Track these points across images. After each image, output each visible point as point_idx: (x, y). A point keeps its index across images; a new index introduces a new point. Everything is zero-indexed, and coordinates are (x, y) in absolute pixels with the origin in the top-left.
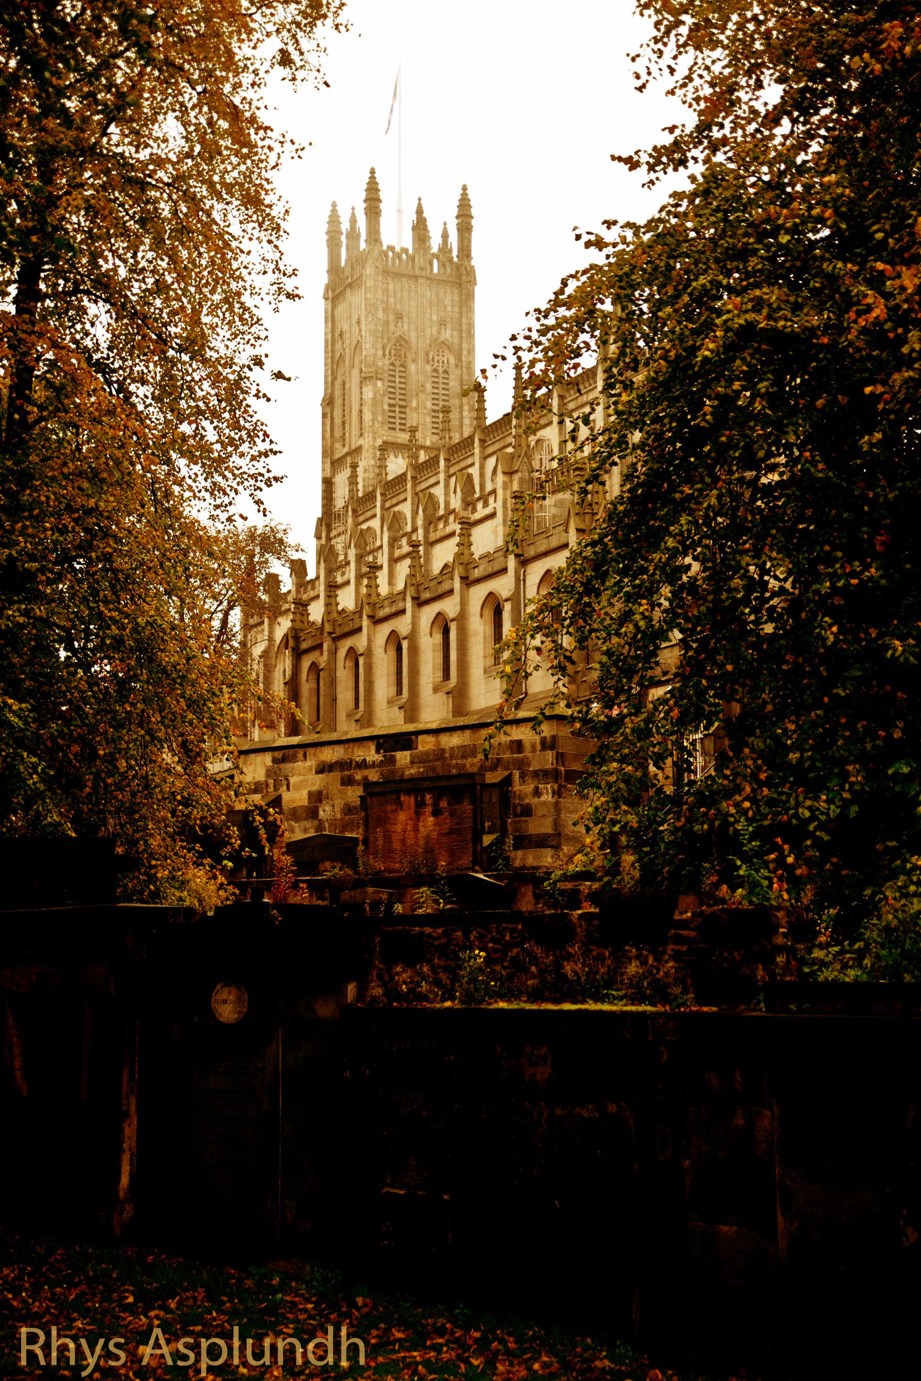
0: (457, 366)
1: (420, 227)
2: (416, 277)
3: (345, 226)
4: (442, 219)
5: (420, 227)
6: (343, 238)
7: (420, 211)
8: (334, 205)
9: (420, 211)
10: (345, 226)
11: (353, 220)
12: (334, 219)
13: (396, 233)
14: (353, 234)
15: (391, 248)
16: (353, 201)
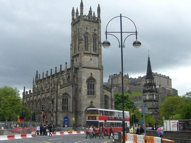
0: (98, 38)
1: (90, 12)
2: (90, 21)
3: (75, 11)
4: (95, 10)
6: (75, 14)
7: (91, 9)
8: (73, 8)
9: (91, 9)
10: (75, 11)
11: (77, 10)
12: (73, 10)
13: (86, 12)
14: (77, 13)
15: (85, 15)
16: (77, 6)
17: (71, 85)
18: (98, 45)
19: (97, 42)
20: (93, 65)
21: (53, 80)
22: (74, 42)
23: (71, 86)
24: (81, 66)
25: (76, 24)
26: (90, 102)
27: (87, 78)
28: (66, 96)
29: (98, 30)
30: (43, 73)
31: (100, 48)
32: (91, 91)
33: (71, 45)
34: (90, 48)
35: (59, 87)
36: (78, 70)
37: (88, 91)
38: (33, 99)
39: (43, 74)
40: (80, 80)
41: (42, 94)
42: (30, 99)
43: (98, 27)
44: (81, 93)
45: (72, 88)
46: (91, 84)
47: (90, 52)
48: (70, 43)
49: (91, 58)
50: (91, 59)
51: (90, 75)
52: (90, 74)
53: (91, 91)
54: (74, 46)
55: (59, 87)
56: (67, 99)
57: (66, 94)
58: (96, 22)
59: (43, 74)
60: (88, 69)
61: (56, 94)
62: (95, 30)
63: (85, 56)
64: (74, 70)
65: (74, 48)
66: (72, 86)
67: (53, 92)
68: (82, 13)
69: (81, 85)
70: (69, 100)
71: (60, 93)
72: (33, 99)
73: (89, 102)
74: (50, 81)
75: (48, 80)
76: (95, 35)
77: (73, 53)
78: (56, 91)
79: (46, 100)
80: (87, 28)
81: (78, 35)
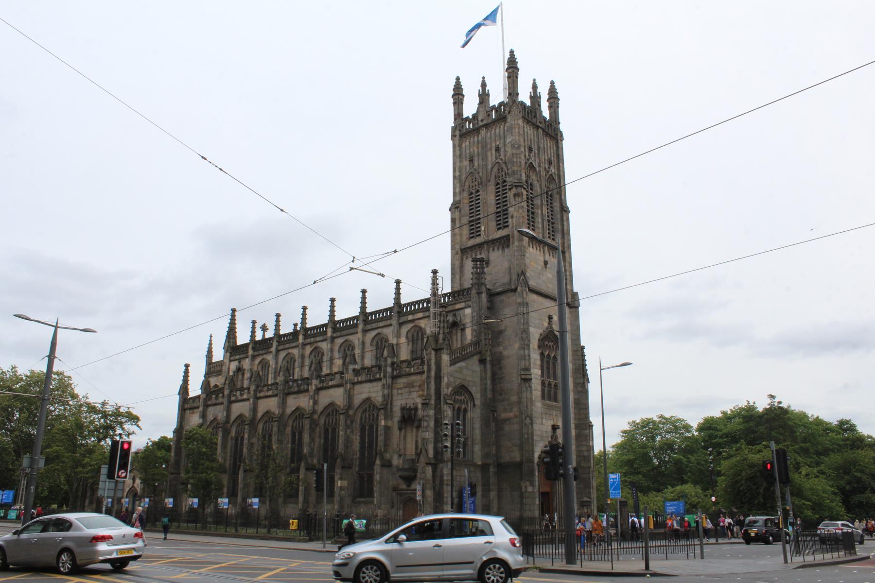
1: (535, 97)
2: (538, 127)
5: (535, 97)
13: (524, 96)
17: (476, 358)
18: (559, 216)
19: (556, 205)
20: (550, 286)
21: (339, 341)
22: (466, 194)
23: (477, 362)
24: (526, 283)
25: (483, 132)
26: (550, 428)
27: (540, 331)
28: (463, 398)
29: (559, 166)
30: (254, 322)
31: (565, 228)
32: (550, 384)
33: (455, 207)
34: (540, 220)
35: (445, 358)
36: (503, 297)
37: (543, 383)
38: (255, 409)
39: (254, 328)
40: (524, 335)
41: (318, 389)
42: (228, 411)
43: (558, 155)
44: (531, 387)
45: (477, 368)
46: (549, 355)
47: (541, 235)
48: (450, 201)
49: (547, 257)
50: (546, 263)
51: (546, 324)
52: (547, 320)
53: (550, 384)
54: (466, 209)
55: (445, 358)
56: (465, 410)
57: (462, 389)
58: (551, 136)
59: (254, 328)
60: (541, 299)
61: (433, 387)
62: (550, 163)
63: (531, 249)
64: (484, 296)
65: (465, 220)
66: (482, 361)
67: (402, 381)
68: (513, 91)
69: (529, 355)
70: (469, 415)
71: (448, 386)
72: (255, 409)
73: (548, 424)
74: (324, 346)
75: (256, 353)
76: (551, 179)
77: (464, 238)
78: (433, 373)
79: (351, 412)
80: (530, 150)
81: (495, 169)
